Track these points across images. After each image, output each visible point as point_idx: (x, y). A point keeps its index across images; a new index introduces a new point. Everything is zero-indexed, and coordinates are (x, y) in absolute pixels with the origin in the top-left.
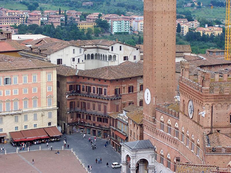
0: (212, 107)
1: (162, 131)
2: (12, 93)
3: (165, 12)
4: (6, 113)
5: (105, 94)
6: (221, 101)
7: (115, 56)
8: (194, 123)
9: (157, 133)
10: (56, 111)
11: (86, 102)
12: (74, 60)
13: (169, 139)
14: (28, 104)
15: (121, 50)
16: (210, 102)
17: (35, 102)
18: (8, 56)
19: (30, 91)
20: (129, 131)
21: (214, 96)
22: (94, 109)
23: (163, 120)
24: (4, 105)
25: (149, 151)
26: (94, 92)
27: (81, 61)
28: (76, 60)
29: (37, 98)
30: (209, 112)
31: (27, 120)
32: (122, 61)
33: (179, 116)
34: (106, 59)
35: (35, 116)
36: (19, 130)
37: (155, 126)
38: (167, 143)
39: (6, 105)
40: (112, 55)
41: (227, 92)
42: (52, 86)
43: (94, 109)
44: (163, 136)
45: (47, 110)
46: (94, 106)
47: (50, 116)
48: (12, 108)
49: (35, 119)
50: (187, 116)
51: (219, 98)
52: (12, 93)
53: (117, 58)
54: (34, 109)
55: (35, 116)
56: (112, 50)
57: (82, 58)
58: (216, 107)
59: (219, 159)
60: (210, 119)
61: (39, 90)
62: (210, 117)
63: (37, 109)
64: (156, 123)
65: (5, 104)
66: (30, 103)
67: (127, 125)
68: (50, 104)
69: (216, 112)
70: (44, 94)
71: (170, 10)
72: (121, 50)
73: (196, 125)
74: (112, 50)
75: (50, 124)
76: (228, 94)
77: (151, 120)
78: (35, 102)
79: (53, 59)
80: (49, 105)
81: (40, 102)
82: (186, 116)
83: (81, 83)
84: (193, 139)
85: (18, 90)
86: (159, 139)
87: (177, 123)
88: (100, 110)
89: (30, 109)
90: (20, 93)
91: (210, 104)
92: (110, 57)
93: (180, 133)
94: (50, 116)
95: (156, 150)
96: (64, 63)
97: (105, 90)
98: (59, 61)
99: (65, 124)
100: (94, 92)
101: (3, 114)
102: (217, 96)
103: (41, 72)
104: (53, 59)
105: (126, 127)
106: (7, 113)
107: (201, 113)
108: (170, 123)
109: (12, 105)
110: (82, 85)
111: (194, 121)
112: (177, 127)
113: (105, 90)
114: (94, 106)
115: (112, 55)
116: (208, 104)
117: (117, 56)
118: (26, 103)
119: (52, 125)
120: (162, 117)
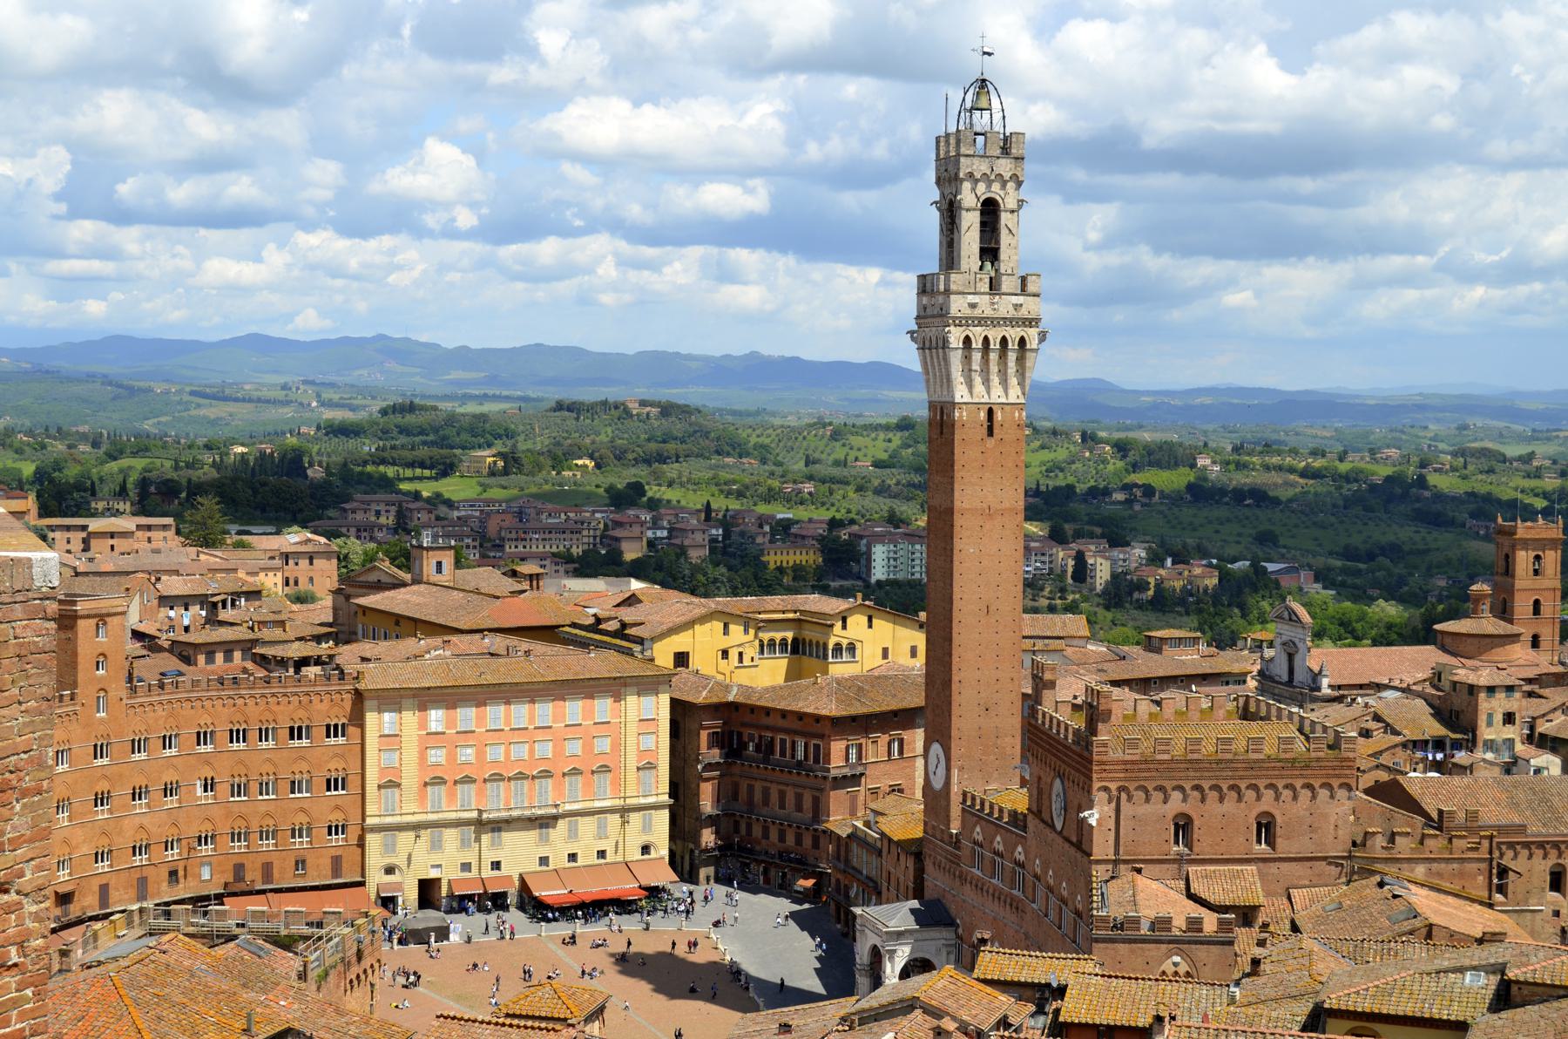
0: (1119, 799)
1: (979, 873)
3: (989, 513)
6: (1146, 779)
7: (852, 648)
8: (1067, 845)
9: (963, 878)
10: (666, 812)
12: (725, 654)
13: (997, 896)
15: (870, 626)
16: (1112, 780)
18: (524, 645)
19: (588, 747)
20: (885, 875)
21: (1126, 762)
22: (782, 806)
23: (980, 838)
24: (508, 790)
25: (937, 935)
26: (783, 754)
27: (747, 662)
28: (733, 655)
30: (1109, 810)
31: (576, 835)
32: (879, 661)
33: (1024, 829)
34: (825, 657)
35: (602, 827)
36: (551, 867)
37: (958, 857)
38: (992, 908)
40: (845, 642)
41: (1164, 752)
43: (782, 806)
44: (979, 886)
46: (782, 795)
47: (647, 827)
48: (531, 798)
49: (601, 834)
50: (1053, 827)
51: (1140, 770)
53: (858, 652)
54: (598, 804)
55: (602, 827)
56: (844, 627)
57: (751, 652)
58: (1130, 798)
59: (1132, 951)
60: (1113, 833)
62: (1112, 825)
63: (607, 804)
64: (958, 848)
67: (880, 853)
69: (1131, 813)
71: (1007, 505)
72: (870, 626)
73: (1073, 850)
74: (844, 627)
75: (646, 849)
76: (1166, 757)
77: (946, 838)
79: (663, 654)
81: (618, 784)
82: (1043, 821)
83: (744, 725)
84: (1065, 893)
86: (969, 894)
87: (1020, 849)
88: (799, 808)
91: (1113, 786)
92: (838, 649)
93: (1030, 878)
94: (647, 827)
95: (960, 931)
96: (695, 662)
97: (817, 747)
98: (681, 659)
99: (692, 851)
100: (783, 754)
102: (1133, 762)
104: (663, 654)
105: (874, 860)
107: (1086, 814)
108: (1001, 848)
109: (530, 790)
110: (747, 732)
111: (1067, 840)
112: (1022, 858)
113: (817, 747)
114: (782, 795)
115: (845, 642)
116: (1106, 789)
117: (858, 645)
120: (978, 829)
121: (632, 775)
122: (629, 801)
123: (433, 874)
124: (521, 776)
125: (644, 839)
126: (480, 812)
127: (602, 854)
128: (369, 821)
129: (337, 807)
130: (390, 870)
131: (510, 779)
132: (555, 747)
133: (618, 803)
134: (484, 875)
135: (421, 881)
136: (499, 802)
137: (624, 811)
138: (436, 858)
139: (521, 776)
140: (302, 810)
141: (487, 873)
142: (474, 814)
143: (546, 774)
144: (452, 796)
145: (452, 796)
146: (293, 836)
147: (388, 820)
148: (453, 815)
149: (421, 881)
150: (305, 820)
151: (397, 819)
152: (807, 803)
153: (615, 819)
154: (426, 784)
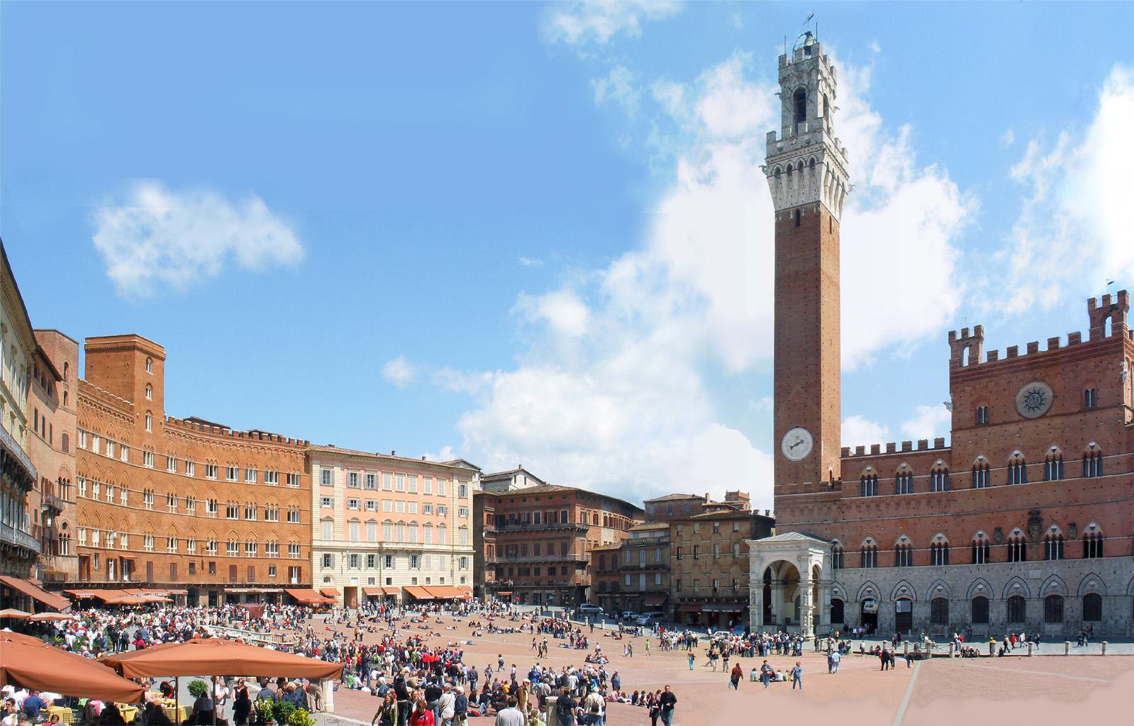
5: (564, 520)
11: (517, 543)
35: (442, 562)
45: (458, 553)
63: (444, 548)
121: (456, 530)
122: (456, 548)
124: (402, 523)
126: (380, 543)
128: (315, 543)
129: (294, 533)
131: (395, 524)
133: (450, 548)
136: (393, 537)
137: (453, 553)
139: (402, 523)
140: (274, 531)
142: (377, 545)
143: (414, 524)
146: (267, 550)
148: (364, 545)
150: (275, 539)
152: (558, 546)
153: (448, 557)
154: (348, 522)
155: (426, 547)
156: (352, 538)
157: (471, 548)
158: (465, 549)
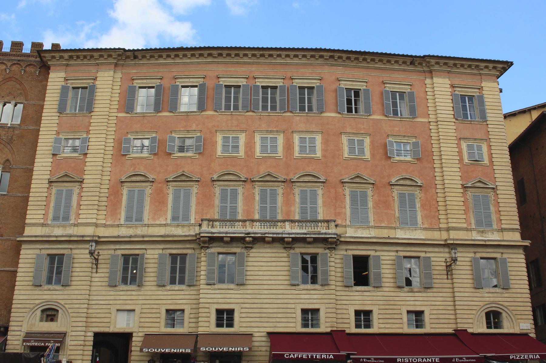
2: (289, 146)
4: (249, 230)
14: (370, 204)
17: (407, 203)
29: (416, 184)
39: (257, 198)
42: (488, 140)
52: (289, 146)
54: (402, 235)
61: (424, 156)
63: (419, 235)
65: (257, 191)
66: (384, 204)
68: (484, 223)
70: (451, 176)
75: (493, 317)
78: (407, 203)
80: (479, 223)
81: (432, 209)
85: (319, 138)
89: (385, 233)
90: (332, 152)
101: (238, 230)
103: (428, 81)
106: (258, 229)
118: (358, 201)
119: (507, 328)
122: (453, 235)
123: (120, 324)
124: (269, 179)
125: (490, 297)
127: (418, 316)
130: (50, 314)
132: (326, 142)
134: (201, 330)
135: (97, 335)
137: (451, 246)
138: (127, 295)
141: (208, 325)
144: (159, 202)
145: (159, 202)
147: (58, 232)
149: (97, 335)
151: (71, 231)
155: (351, 233)
156: (128, 218)
157: (516, 237)
158: (493, 237)
